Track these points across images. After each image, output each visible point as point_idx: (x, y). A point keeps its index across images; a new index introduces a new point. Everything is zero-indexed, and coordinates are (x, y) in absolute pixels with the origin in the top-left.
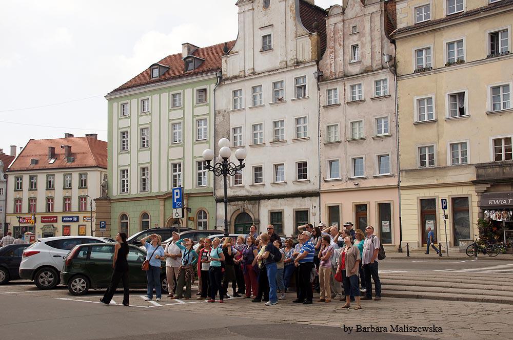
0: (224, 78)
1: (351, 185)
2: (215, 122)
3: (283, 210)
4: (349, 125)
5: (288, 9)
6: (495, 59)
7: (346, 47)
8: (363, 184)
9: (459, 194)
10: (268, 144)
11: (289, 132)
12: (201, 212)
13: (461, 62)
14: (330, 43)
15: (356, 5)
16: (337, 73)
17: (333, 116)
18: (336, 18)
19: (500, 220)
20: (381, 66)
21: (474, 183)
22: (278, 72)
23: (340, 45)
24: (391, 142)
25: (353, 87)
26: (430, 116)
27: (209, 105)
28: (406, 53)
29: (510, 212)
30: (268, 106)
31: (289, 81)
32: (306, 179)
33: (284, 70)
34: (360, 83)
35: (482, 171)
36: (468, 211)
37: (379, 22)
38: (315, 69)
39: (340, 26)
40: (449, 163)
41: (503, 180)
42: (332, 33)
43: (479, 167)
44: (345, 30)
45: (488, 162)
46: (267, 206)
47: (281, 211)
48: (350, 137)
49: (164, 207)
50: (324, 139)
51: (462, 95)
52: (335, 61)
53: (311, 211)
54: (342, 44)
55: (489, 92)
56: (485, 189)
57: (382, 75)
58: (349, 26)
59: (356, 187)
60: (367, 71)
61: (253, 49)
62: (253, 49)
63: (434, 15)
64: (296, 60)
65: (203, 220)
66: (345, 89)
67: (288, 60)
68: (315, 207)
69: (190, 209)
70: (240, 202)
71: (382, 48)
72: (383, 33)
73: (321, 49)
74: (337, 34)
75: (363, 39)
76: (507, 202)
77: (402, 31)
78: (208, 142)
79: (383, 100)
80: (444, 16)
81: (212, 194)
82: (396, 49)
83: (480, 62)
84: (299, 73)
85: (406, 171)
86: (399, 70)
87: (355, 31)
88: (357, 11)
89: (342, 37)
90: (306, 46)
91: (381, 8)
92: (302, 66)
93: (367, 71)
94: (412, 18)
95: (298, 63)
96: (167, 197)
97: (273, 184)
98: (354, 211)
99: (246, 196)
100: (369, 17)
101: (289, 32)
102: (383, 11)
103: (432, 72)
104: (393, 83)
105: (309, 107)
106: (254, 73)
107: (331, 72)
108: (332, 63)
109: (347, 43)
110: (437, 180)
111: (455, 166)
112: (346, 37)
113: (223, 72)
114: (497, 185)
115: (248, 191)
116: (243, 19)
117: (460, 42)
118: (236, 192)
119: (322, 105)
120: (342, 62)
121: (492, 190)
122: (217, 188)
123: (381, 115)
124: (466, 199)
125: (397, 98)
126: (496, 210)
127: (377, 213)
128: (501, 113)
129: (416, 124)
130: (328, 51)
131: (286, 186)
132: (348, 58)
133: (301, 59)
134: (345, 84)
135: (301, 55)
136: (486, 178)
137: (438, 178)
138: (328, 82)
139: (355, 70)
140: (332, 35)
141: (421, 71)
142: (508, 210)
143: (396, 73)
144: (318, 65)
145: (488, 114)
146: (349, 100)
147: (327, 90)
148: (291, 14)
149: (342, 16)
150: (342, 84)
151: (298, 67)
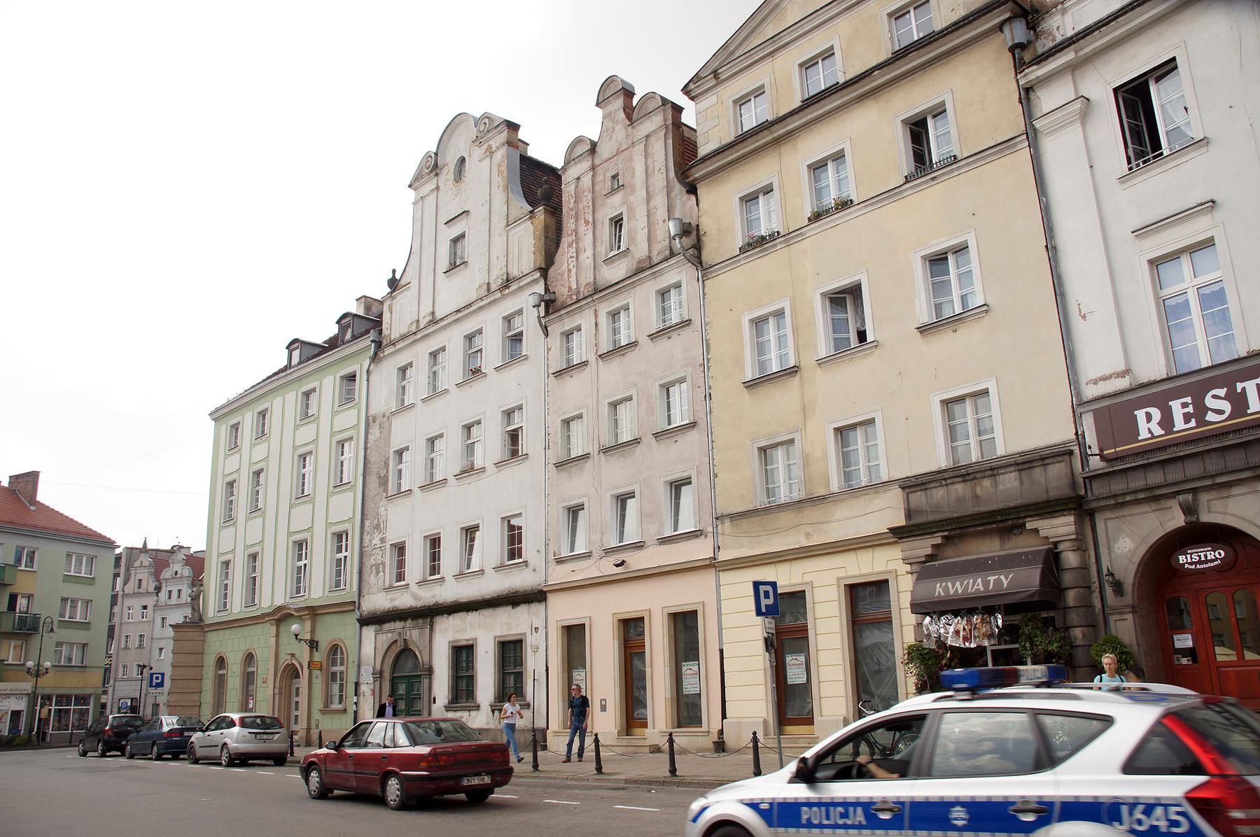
0: (385, 342)
1: (607, 568)
2: (366, 442)
3: (476, 639)
4: (605, 409)
5: (495, 172)
6: (925, 182)
7: (599, 227)
8: (638, 562)
9: (864, 571)
10: (452, 480)
12: (337, 649)
13: (844, 205)
14: (569, 224)
15: (616, 128)
16: (582, 289)
18: (579, 166)
19: (973, 645)
20: (667, 253)
21: (899, 534)
22: (471, 309)
23: (587, 222)
27: (358, 406)
29: (996, 618)
30: (454, 391)
31: (491, 323)
32: (521, 560)
33: (483, 303)
34: (625, 302)
35: (918, 498)
36: (889, 621)
38: (540, 288)
39: (586, 180)
40: (835, 485)
41: (973, 517)
42: (572, 201)
43: (911, 485)
44: (597, 188)
45: (933, 468)
46: (447, 630)
47: (470, 643)
48: (607, 441)
49: (277, 642)
50: (556, 454)
51: (854, 292)
53: (530, 642)
54: (590, 219)
55: (919, 270)
56: (929, 551)
58: (605, 176)
59: (620, 570)
60: (644, 268)
61: (434, 270)
62: (434, 270)
63: (775, 107)
64: (505, 277)
65: (337, 669)
66: (596, 325)
68: (536, 629)
69: (317, 642)
70: (398, 625)
72: (672, 174)
74: (582, 201)
75: (632, 199)
76: (986, 583)
78: (353, 488)
79: (674, 335)
80: (797, 104)
81: (354, 605)
82: (698, 205)
83: (891, 194)
85: (736, 517)
86: (709, 255)
87: (616, 183)
88: (619, 140)
89: (590, 204)
91: (665, 120)
93: (644, 268)
94: (729, 124)
96: (281, 617)
97: (460, 576)
98: (616, 636)
99: (412, 608)
100: (642, 146)
101: (495, 218)
102: (671, 127)
103: (781, 243)
104: (696, 287)
106: (434, 322)
107: (570, 289)
108: (571, 267)
109: (599, 215)
110: (808, 535)
111: (852, 491)
112: (599, 201)
113: (385, 332)
114: (962, 537)
115: (415, 597)
116: (420, 212)
117: (839, 157)
118: (395, 599)
119: (552, 371)
120: (591, 259)
121: (949, 551)
122: (365, 590)
123: (673, 374)
124: (881, 586)
125: (704, 325)
126: (956, 613)
127: (666, 638)
128: (957, 320)
130: (565, 241)
131: (483, 579)
132: (603, 249)
133: (515, 272)
134: (596, 311)
135: (516, 263)
136: (931, 518)
137: (809, 529)
138: (563, 312)
140: (572, 205)
141: (757, 244)
142: (990, 611)
143: (701, 263)
144: (546, 280)
145: (924, 330)
146: (605, 347)
147: (562, 333)
148: (499, 179)
149: (590, 159)
151: (507, 291)
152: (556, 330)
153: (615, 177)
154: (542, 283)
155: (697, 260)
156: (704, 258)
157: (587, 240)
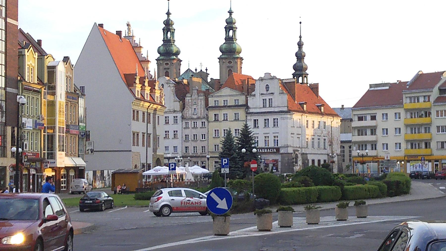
11: (171, 135)
14: (186, 106)
17: (187, 132)
23: (190, 107)
24: (206, 142)
25: (194, 123)
26: (218, 135)
28: (211, 114)
31: (171, 117)
37: (203, 103)
39: (190, 101)
52: (189, 112)
67: (171, 109)
71: (204, 111)
73: (183, 107)
77: (210, 107)
83: (232, 121)
84: (175, 115)
85: (211, 152)
90: (177, 106)
92: (176, 112)
95: (175, 111)
105: (179, 127)
107: (187, 116)
119: (183, 127)
120: (190, 113)
129: (214, 138)
130: (185, 109)
139: (195, 117)
150: (190, 121)
152: (184, 122)
153: (195, 102)
154: (181, 114)
155: (208, 120)
156: (209, 120)
157: (190, 110)
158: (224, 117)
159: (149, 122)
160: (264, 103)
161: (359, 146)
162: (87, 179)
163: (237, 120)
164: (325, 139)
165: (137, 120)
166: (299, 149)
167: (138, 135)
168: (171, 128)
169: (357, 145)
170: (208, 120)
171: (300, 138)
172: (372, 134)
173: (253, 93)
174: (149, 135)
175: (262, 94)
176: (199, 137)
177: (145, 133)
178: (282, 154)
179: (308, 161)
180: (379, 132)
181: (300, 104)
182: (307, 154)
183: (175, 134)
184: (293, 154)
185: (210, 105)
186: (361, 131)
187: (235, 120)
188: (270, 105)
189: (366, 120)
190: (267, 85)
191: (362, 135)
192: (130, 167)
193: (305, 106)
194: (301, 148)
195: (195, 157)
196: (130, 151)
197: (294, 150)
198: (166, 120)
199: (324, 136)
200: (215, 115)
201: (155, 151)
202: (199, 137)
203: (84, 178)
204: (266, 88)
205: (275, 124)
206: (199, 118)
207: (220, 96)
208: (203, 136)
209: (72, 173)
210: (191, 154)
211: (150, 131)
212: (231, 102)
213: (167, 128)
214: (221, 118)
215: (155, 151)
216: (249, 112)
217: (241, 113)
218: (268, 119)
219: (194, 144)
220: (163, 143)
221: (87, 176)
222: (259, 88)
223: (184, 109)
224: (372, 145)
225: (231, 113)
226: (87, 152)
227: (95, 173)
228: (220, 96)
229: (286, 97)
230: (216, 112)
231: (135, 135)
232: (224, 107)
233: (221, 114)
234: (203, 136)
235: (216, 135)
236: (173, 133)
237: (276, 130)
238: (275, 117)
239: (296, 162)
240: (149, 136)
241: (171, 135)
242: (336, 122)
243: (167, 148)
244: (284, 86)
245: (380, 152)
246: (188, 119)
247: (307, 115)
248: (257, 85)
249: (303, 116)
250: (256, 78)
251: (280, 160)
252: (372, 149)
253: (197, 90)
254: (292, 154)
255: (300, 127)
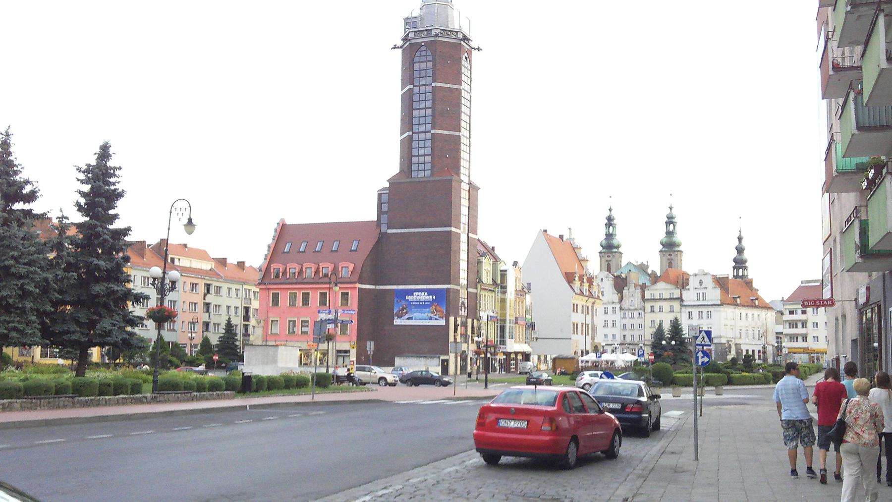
11: (610, 324)
14: (624, 298)
17: (625, 321)
28: (648, 306)
37: (640, 295)
52: (626, 304)
57: (640, 311)
73: (621, 299)
77: (646, 300)
84: (614, 306)
90: (616, 298)
95: (613, 303)
105: (617, 317)
129: (650, 327)
130: (623, 300)
139: (633, 308)
152: (622, 312)
158: (660, 309)
159: (587, 313)
160: (697, 297)
161: (790, 338)
162: (533, 362)
163: (672, 311)
164: (759, 331)
165: (577, 312)
166: (733, 340)
167: (577, 325)
168: (610, 317)
169: (788, 338)
170: (644, 311)
171: (734, 329)
172: (803, 327)
173: (687, 287)
174: (587, 326)
175: (696, 288)
176: (636, 326)
177: (583, 324)
178: (715, 344)
179: (742, 350)
180: (809, 325)
181: (733, 298)
182: (740, 344)
183: (613, 324)
184: (726, 345)
185: (646, 298)
186: (793, 324)
187: (671, 311)
188: (703, 299)
189: (796, 314)
190: (701, 280)
191: (793, 328)
192: (571, 354)
193: (738, 300)
194: (735, 339)
195: (632, 344)
196: (571, 339)
197: (727, 341)
198: (605, 311)
199: (758, 328)
200: (651, 307)
201: (593, 338)
202: (636, 326)
203: (530, 361)
204: (700, 283)
205: (709, 315)
206: (636, 309)
207: (656, 290)
208: (640, 326)
209: (520, 357)
210: (628, 342)
211: (589, 322)
212: (666, 295)
213: (606, 317)
214: (657, 309)
215: (593, 338)
216: (683, 304)
217: (676, 305)
218: (702, 312)
219: (632, 333)
220: (601, 331)
221: (533, 359)
222: (693, 283)
223: (621, 301)
224: (803, 338)
225: (666, 305)
226: (532, 339)
227: (539, 357)
228: (656, 290)
229: (718, 292)
230: (653, 304)
231: (575, 325)
232: (660, 299)
233: (657, 306)
234: (640, 326)
235: (652, 325)
236: (612, 322)
237: (709, 321)
238: (709, 309)
239: (730, 352)
240: (588, 326)
241: (610, 324)
242: (771, 316)
243: (606, 336)
244: (719, 282)
245: (811, 344)
246: (626, 310)
247: (740, 308)
248: (691, 279)
249: (736, 309)
250: (690, 273)
251: (713, 349)
252: (803, 341)
253: (634, 284)
254: (725, 344)
255: (733, 319)
